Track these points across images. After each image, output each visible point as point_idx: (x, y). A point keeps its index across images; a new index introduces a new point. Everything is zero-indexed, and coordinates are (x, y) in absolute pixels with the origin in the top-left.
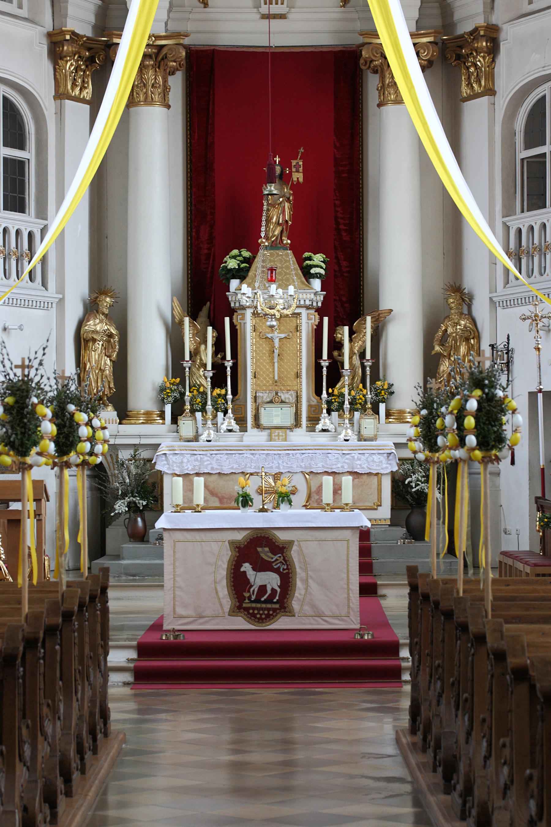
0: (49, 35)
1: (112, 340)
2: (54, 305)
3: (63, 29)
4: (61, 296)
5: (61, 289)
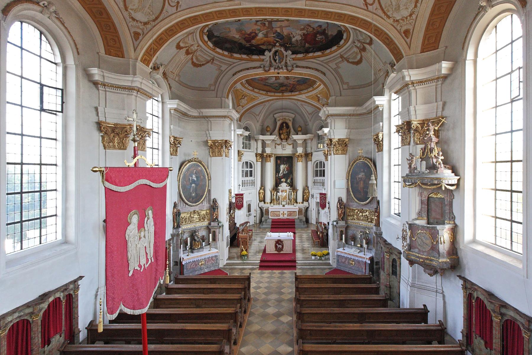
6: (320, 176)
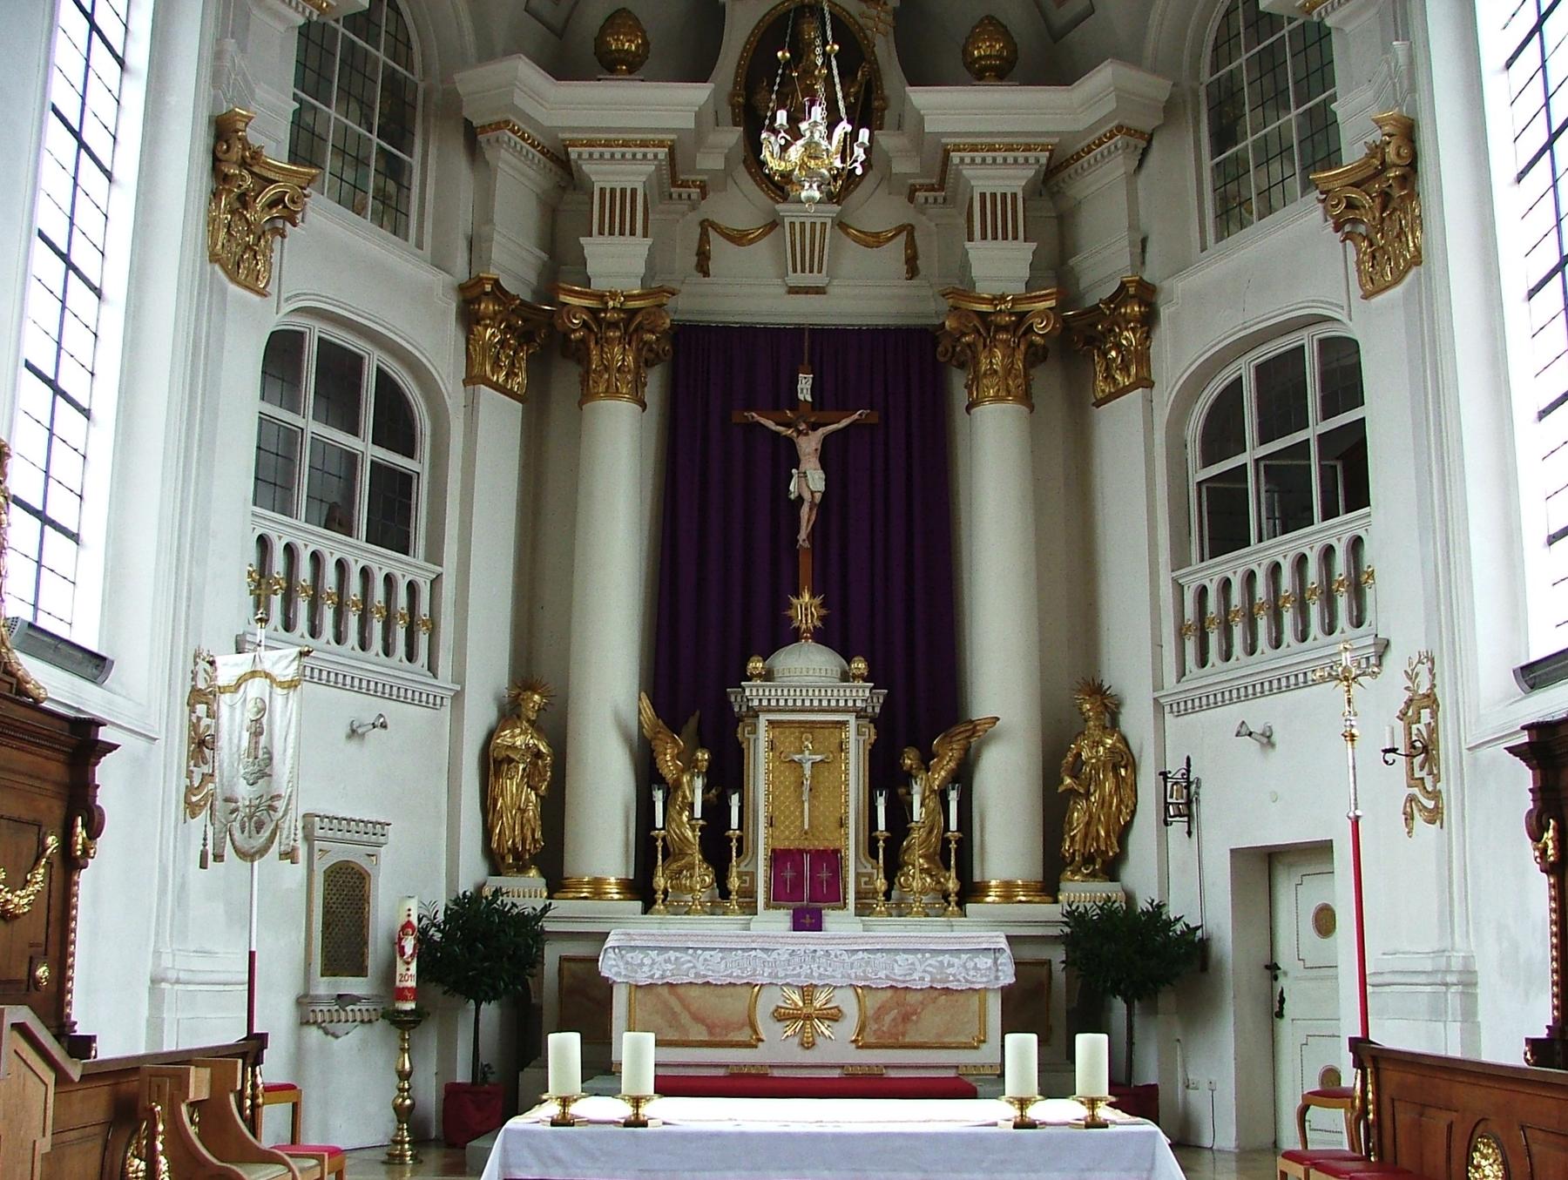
0: (462, 288)
1: (540, 762)
2: (447, 702)
3: (481, 275)
4: (458, 688)
5: (459, 677)
6: (1293, 516)
